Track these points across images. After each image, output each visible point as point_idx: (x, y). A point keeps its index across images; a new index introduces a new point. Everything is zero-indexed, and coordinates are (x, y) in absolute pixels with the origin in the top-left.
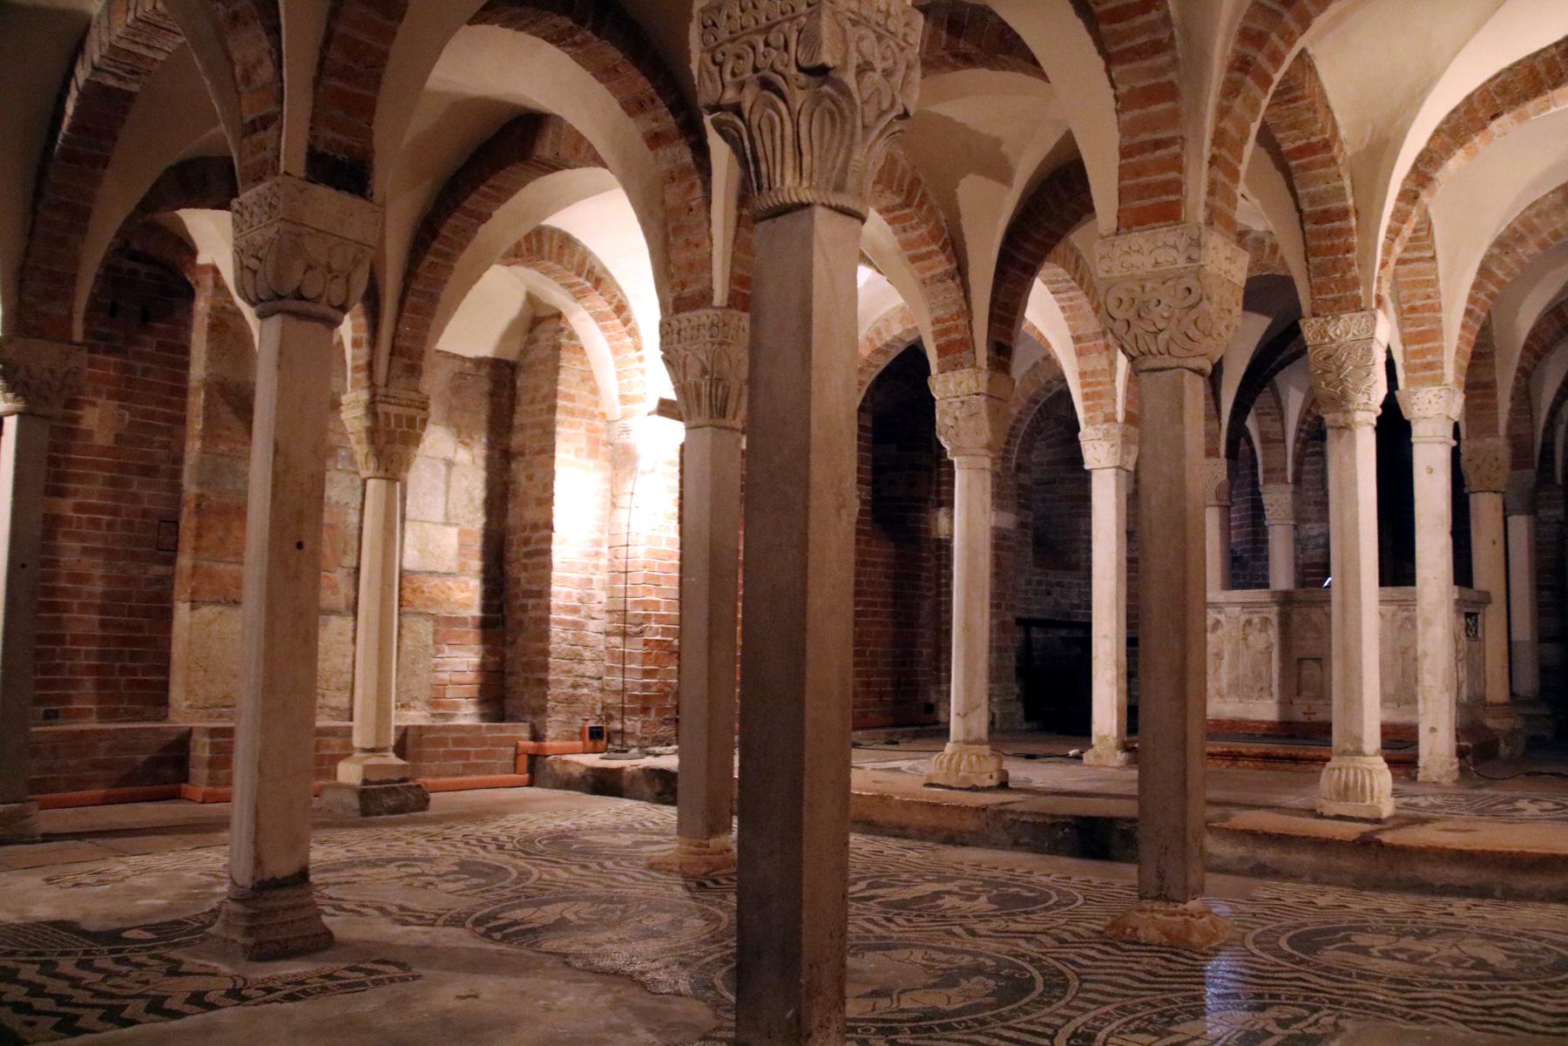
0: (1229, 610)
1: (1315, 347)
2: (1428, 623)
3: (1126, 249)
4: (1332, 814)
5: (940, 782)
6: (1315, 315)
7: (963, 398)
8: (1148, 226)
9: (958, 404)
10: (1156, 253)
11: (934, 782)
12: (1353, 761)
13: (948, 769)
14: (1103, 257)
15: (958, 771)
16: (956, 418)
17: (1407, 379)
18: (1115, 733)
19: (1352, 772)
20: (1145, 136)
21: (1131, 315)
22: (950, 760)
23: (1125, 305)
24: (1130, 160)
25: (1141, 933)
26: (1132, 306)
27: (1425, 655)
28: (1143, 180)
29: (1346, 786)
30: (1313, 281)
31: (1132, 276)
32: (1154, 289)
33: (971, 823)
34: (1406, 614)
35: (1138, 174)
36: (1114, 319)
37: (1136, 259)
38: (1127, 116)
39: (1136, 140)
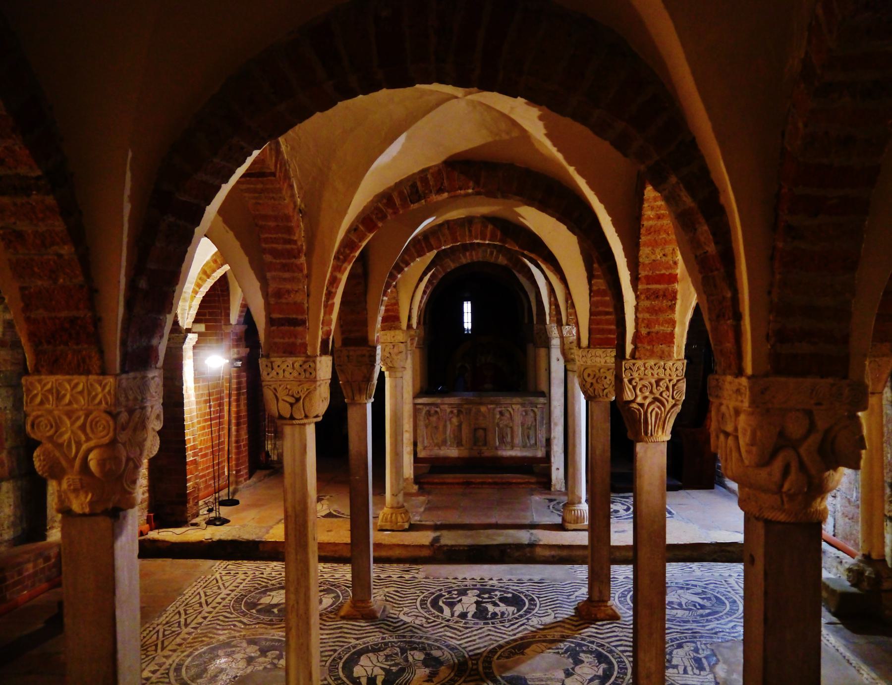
0: (442, 407)
1: (566, 337)
2: (556, 424)
3: (593, 354)
4: (572, 528)
5: (389, 528)
6: (568, 324)
7: (393, 344)
8: (602, 347)
9: (392, 347)
10: (607, 358)
11: (384, 528)
12: (578, 506)
13: (391, 522)
14: (583, 356)
15: (397, 523)
16: (390, 353)
17: (550, 320)
18: (412, 477)
19: (579, 512)
20: (601, 309)
21: (594, 381)
22: (391, 517)
23: (592, 376)
24: (595, 317)
25: (598, 616)
26: (593, 378)
27: (554, 438)
28: (601, 327)
29: (577, 517)
30: (569, 310)
31: (595, 366)
32: (604, 372)
33: (425, 553)
34: (523, 409)
35: (598, 324)
36: (586, 382)
37: (598, 359)
38: (595, 299)
39: (598, 309)
